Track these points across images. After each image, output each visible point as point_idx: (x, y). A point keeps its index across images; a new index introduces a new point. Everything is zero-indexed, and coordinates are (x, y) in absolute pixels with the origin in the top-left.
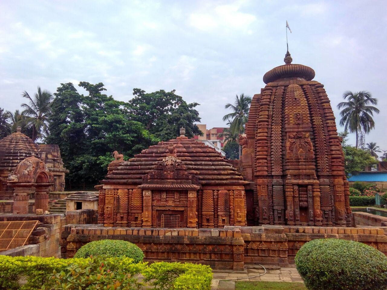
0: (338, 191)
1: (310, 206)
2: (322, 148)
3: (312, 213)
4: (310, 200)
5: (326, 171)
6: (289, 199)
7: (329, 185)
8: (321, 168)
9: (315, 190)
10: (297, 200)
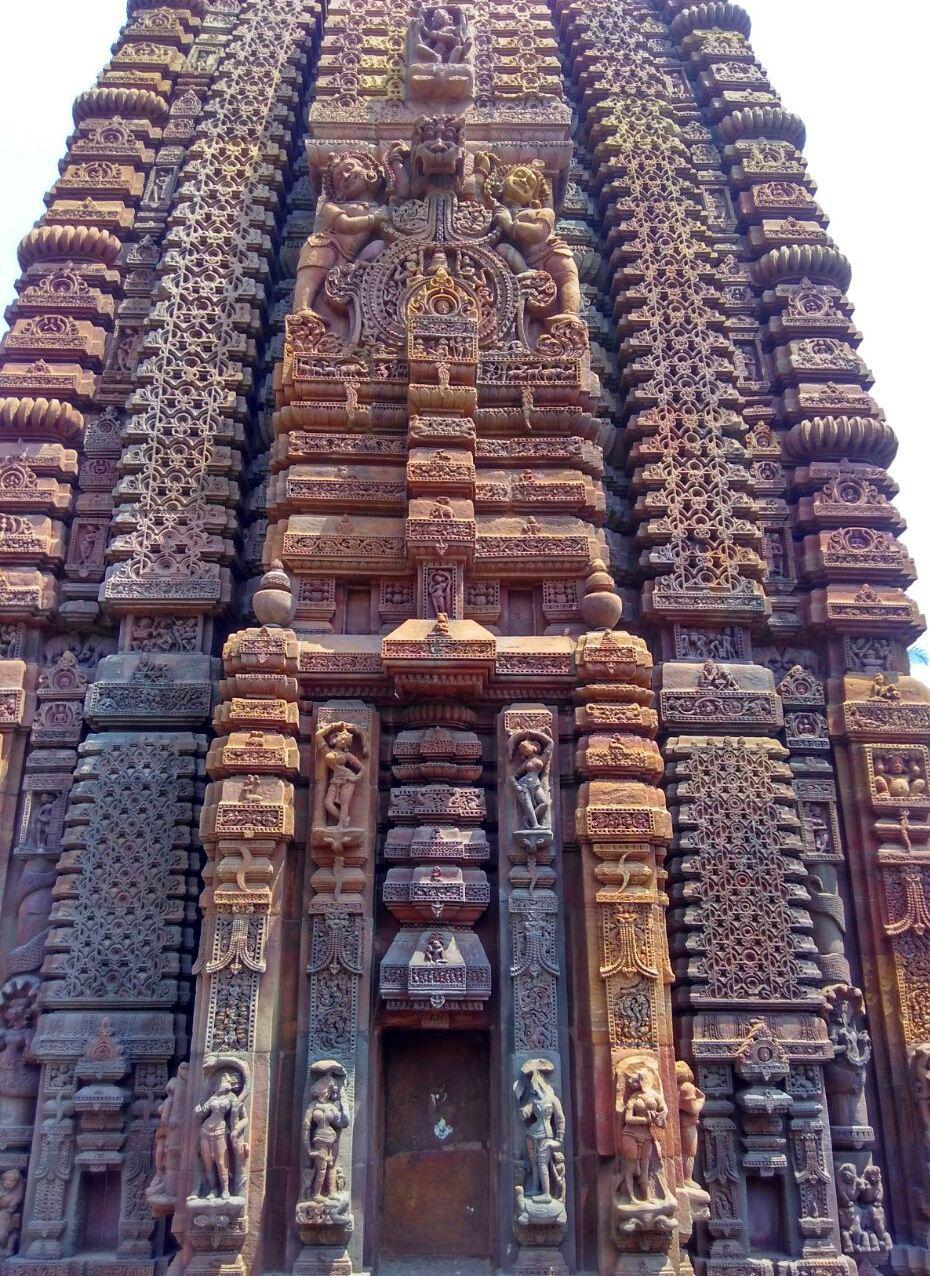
0: (894, 814)
1: (520, 999)
2: (680, 344)
3: (549, 1097)
4: (532, 906)
5: (731, 565)
6: (246, 890)
7: (780, 734)
8: (679, 533)
9: (598, 748)
10: (344, 894)
